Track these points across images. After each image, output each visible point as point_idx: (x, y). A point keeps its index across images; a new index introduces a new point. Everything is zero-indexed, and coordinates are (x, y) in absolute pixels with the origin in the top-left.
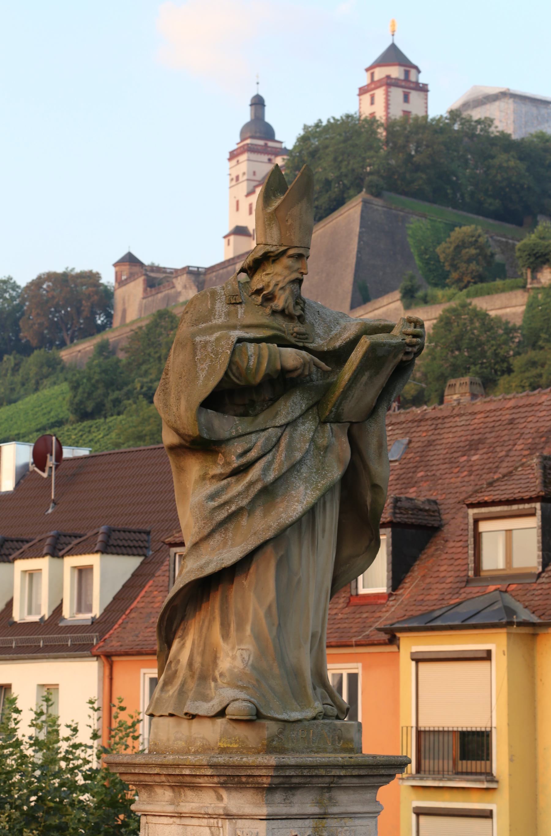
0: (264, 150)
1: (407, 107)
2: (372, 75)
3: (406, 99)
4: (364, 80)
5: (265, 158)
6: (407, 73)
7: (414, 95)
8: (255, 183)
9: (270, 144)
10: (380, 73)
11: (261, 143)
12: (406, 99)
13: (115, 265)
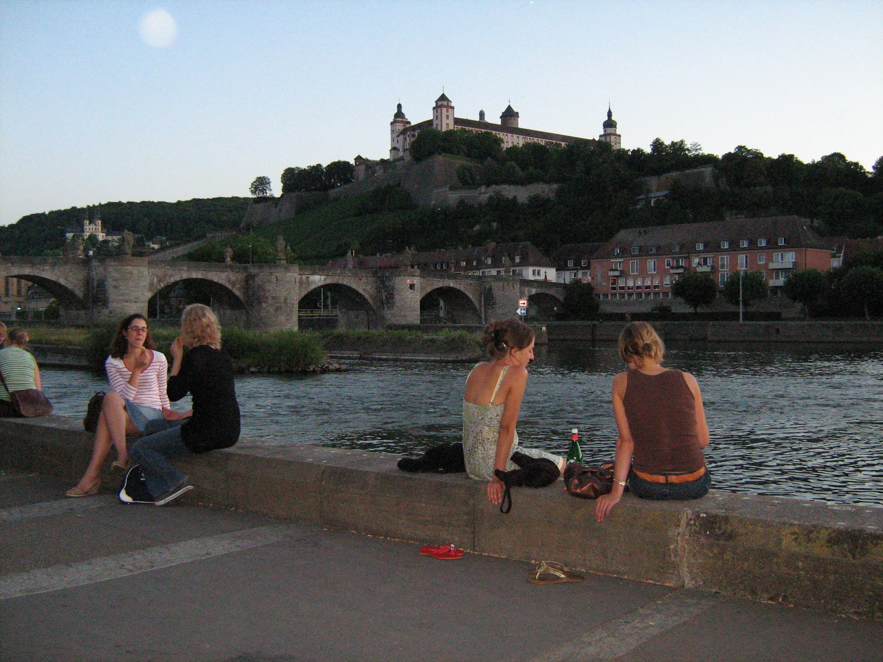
0: (402, 122)
1: (448, 114)
2: (437, 104)
3: (447, 111)
4: (434, 105)
5: (402, 124)
6: (448, 103)
7: (450, 110)
8: (398, 133)
9: (404, 120)
10: (440, 103)
11: (400, 119)
12: (447, 111)
13: (355, 159)
